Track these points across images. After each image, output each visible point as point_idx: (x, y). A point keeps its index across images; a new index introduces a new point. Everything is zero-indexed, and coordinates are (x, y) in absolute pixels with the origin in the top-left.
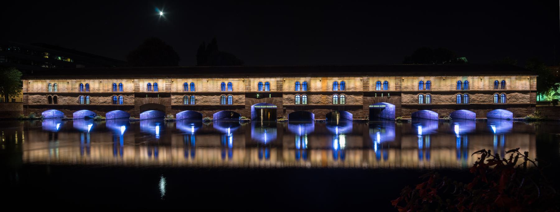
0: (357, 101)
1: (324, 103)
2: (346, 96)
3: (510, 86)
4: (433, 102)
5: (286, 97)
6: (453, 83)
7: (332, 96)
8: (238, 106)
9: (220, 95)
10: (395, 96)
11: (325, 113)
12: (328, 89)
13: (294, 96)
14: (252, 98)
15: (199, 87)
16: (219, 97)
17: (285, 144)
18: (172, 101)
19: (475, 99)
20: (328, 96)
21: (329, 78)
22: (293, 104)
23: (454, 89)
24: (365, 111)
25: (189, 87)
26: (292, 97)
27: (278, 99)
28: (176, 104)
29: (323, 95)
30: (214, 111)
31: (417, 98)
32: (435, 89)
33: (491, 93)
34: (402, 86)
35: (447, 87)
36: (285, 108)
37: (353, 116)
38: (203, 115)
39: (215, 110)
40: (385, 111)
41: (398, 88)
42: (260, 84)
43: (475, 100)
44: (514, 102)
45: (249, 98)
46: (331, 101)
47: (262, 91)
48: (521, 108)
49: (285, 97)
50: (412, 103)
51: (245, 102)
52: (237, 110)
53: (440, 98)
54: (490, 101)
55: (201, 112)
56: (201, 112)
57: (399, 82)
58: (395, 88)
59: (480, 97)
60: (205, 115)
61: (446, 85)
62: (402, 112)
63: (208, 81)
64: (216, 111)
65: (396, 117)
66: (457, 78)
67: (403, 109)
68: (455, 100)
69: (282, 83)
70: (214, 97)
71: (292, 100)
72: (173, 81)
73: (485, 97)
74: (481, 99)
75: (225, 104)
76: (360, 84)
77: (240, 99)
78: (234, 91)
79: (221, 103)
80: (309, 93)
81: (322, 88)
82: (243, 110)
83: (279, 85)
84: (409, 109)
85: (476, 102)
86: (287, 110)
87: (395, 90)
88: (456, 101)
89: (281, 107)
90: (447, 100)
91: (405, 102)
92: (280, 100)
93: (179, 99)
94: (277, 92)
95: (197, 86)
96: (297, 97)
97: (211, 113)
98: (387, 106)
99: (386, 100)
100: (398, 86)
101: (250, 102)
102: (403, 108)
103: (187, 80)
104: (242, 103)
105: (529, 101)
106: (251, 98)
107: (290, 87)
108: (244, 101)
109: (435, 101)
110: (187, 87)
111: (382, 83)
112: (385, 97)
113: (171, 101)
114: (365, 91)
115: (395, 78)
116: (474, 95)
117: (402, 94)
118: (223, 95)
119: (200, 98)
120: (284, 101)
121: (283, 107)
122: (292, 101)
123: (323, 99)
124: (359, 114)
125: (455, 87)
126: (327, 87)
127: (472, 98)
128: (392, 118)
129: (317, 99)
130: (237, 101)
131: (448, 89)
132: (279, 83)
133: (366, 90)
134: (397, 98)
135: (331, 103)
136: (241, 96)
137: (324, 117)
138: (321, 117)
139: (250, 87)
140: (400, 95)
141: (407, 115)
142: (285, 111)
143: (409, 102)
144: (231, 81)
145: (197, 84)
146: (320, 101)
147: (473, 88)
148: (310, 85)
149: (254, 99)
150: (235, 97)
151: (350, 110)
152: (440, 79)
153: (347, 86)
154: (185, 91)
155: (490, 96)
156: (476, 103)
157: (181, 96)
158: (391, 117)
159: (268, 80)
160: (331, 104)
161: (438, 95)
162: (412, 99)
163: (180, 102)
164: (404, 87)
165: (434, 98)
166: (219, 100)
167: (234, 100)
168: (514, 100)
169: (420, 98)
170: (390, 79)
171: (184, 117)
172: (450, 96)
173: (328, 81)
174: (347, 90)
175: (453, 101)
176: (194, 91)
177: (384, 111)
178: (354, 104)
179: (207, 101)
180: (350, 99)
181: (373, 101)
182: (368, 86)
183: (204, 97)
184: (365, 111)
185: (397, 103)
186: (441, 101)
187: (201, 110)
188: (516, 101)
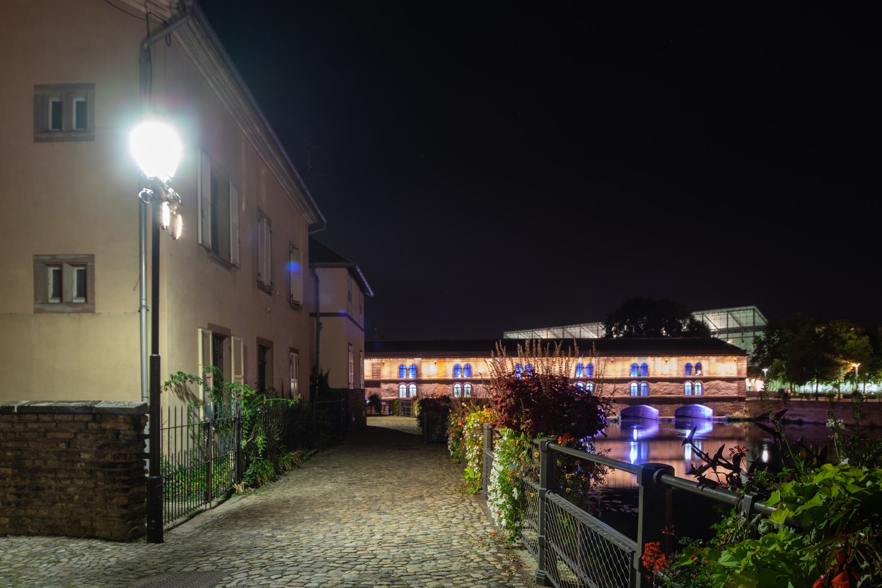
3: (709, 372)
6: (625, 367)
12: (446, 376)
13: (397, 385)
19: (657, 390)
20: (447, 386)
21: (447, 360)
26: (394, 387)
33: (681, 381)
35: (617, 372)
43: (657, 392)
44: (714, 393)
48: (725, 403)
49: (384, 386)
54: (679, 393)
59: (665, 387)
61: (615, 370)
68: (628, 391)
69: (379, 366)
73: (672, 386)
74: (665, 389)
80: (419, 382)
81: (438, 374)
83: (376, 369)
88: (630, 393)
105: (737, 392)
107: (391, 373)
122: (394, 394)
126: (445, 372)
131: (619, 375)
147: (654, 375)
148: (420, 370)
155: (679, 386)
156: (658, 395)
168: (714, 391)
173: (447, 364)
174: (474, 378)
175: (625, 393)
188: (717, 393)
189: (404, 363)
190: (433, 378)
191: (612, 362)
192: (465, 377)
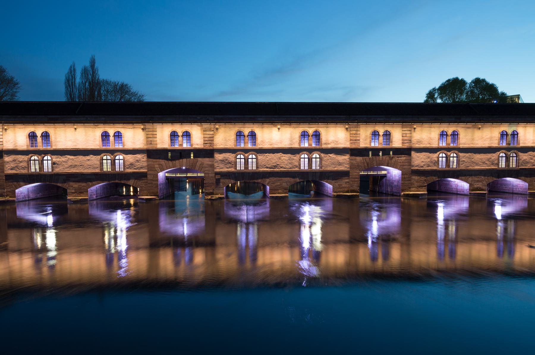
0: (340, 164)
1: (285, 168)
2: (322, 155)
4: (462, 166)
5: (220, 158)
6: (493, 135)
7: (298, 156)
8: (134, 173)
9: (100, 155)
10: (402, 155)
11: (287, 185)
13: (234, 155)
14: (160, 159)
15: (58, 140)
16: (99, 157)
17: (219, 239)
18: (7, 166)
22: (232, 170)
23: (495, 144)
24: (353, 180)
25: (39, 139)
27: (206, 161)
28: (14, 172)
29: (284, 154)
30: (90, 184)
31: (436, 159)
32: (464, 144)
34: (413, 139)
35: (485, 140)
36: (218, 177)
37: (333, 188)
38: (68, 191)
39: (91, 182)
40: (386, 180)
41: (406, 142)
42: (174, 135)
43: (527, 163)
45: (154, 160)
46: (297, 164)
47: (177, 147)
49: (218, 157)
50: (428, 167)
51: (148, 166)
52: (134, 180)
53: (473, 159)
55: (65, 186)
56: (65, 186)
57: (409, 132)
58: (401, 142)
60: (73, 191)
61: (482, 138)
62: (412, 181)
63: (76, 129)
64: (94, 183)
65: (403, 191)
66: (500, 127)
67: (414, 177)
68: (496, 162)
69: (212, 133)
70: (88, 158)
71: (230, 163)
72: (6, 129)
75: (109, 170)
76: (346, 135)
77: (137, 160)
78: (125, 147)
79: (102, 168)
82: (143, 181)
83: (208, 136)
84: (423, 177)
85: (529, 165)
86: (222, 180)
87: (401, 146)
88: (498, 164)
89: (210, 175)
90: (484, 163)
91: (417, 166)
92: (210, 163)
93: (21, 162)
94: (205, 148)
95: (56, 138)
96: (239, 157)
97: (83, 186)
98: (388, 173)
99: (386, 162)
100: (406, 138)
101: (157, 166)
102: (414, 175)
103: (35, 128)
104: (141, 168)
106: (158, 160)
108: (145, 164)
109: (464, 163)
110: (36, 140)
111: (381, 133)
112: (384, 157)
113: (3, 166)
114: (354, 146)
115: (401, 126)
116: (526, 154)
117: (413, 154)
118: (106, 154)
119: (60, 160)
120: (216, 165)
121: (215, 175)
123: (284, 161)
124: (343, 186)
125: (497, 142)
127: (522, 159)
128: (396, 192)
129: (274, 161)
130: (131, 164)
132: (208, 133)
133: (355, 145)
134: (404, 158)
135: (297, 167)
136: (139, 156)
137: (285, 191)
138: (280, 191)
139: (155, 139)
140: (410, 155)
141: (420, 187)
142: (218, 182)
143: (424, 165)
144: (119, 130)
145: (55, 133)
146: (278, 165)
147: (524, 143)
149: (162, 162)
150: (128, 158)
151: (328, 179)
152: (474, 127)
153: (324, 138)
154: (32, 148)
156: (529, 166)
157: (23, 157)
158: (394, 190)
159: (187, 127)
160: (297, 169)
161: (470, 154)
162: (429, 160)
163: (23, 168)
164: (415, 141)
165: (463, 159)
166: (98, 163)
167: (127, 163)
169: (440, 159)
170: (393, 127)
171: (32, 196)
172: (489, 156)
174: (324, 146)
175: (493, 164)
176: (49, 148)
177: (384, 180)
178: (335, 169)
179: (76, 165)
180: (329, 161)
181: (366, 164)
182: (358, 138)
183: (69, 159)
184: (353, 180)
185: (404, 167)
186: (475, 164)
187: (65, 181)
189: (242, 129)
190: (276, 146)
191: (479, 128)
192: (314, 145)
